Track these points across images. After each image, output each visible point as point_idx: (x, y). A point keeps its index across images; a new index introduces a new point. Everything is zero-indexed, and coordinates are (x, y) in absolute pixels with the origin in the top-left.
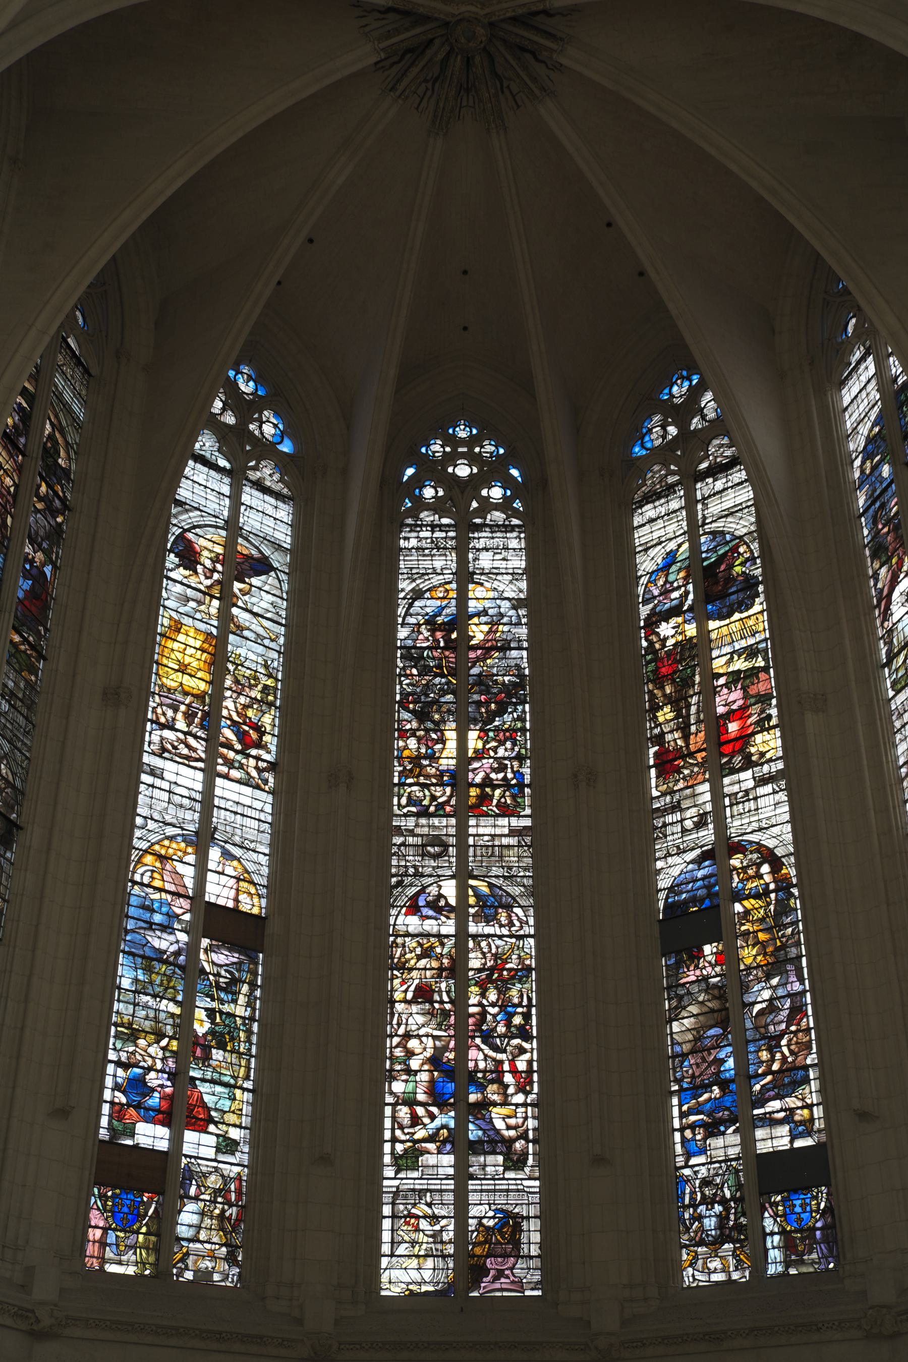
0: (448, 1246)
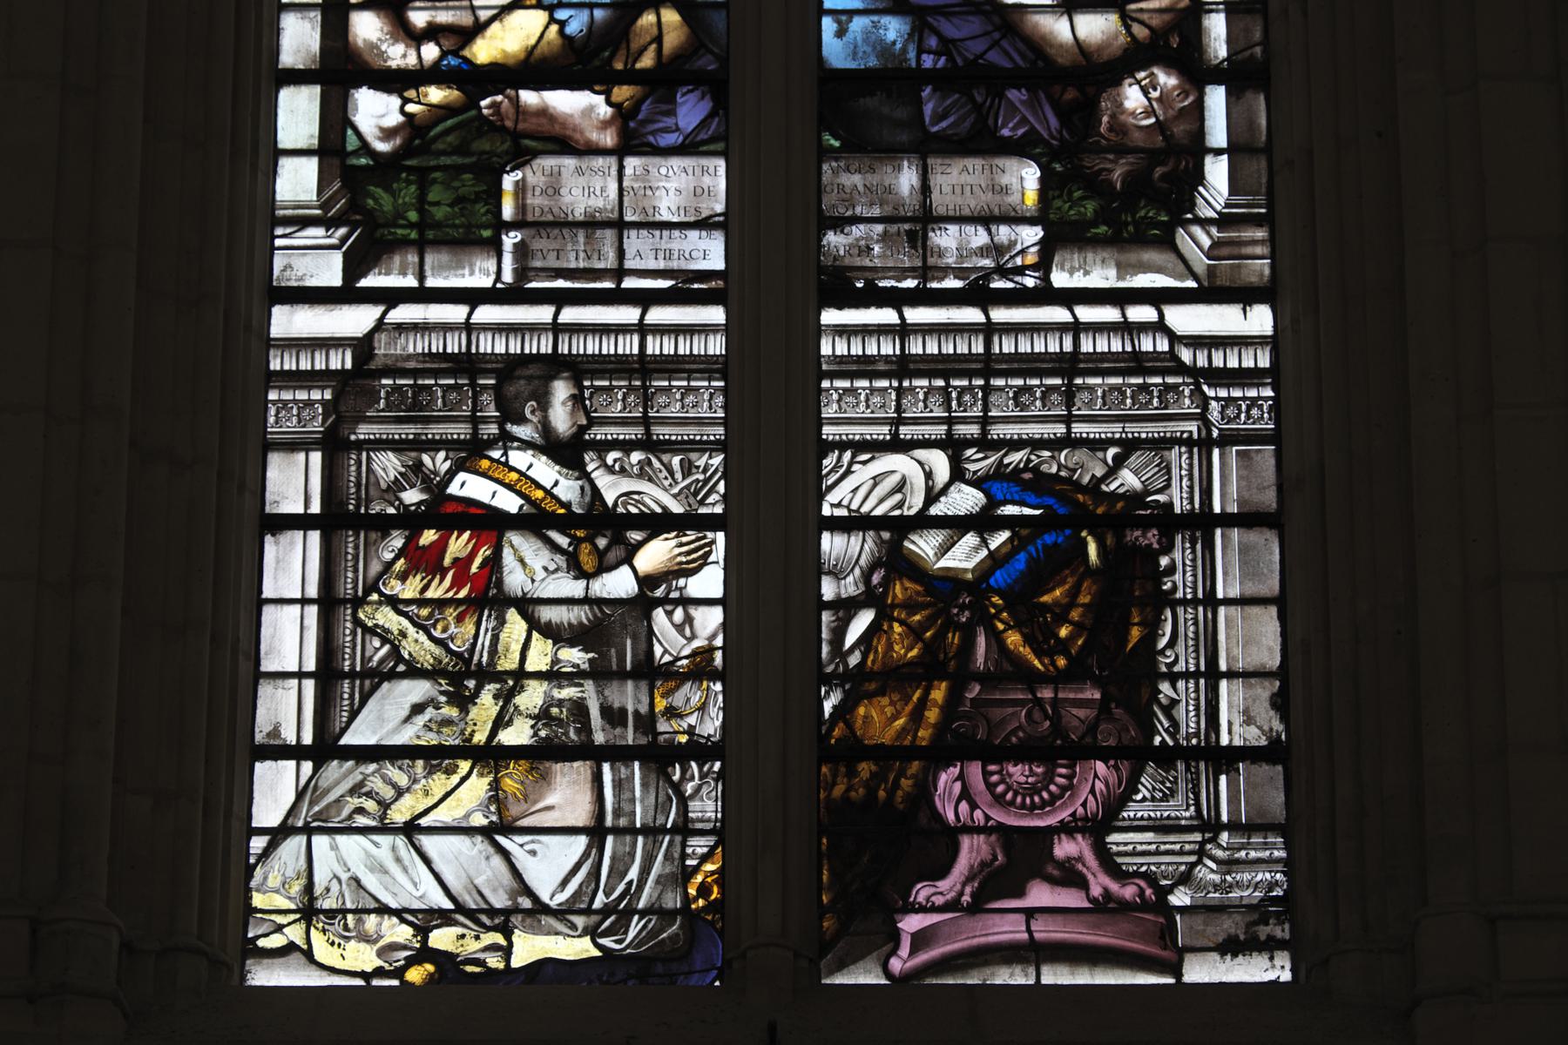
0: (689, 695)
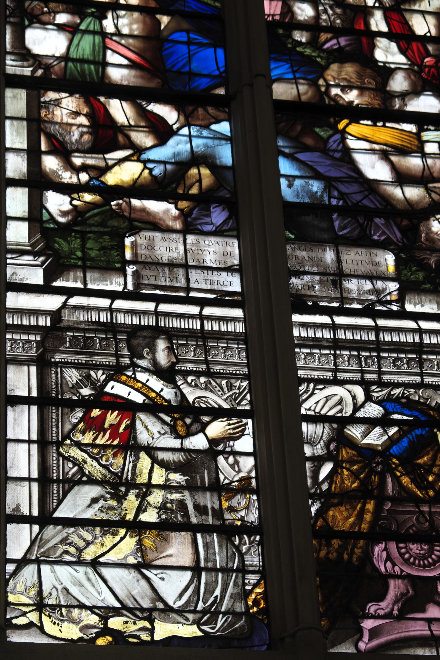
0: (240, 501)
